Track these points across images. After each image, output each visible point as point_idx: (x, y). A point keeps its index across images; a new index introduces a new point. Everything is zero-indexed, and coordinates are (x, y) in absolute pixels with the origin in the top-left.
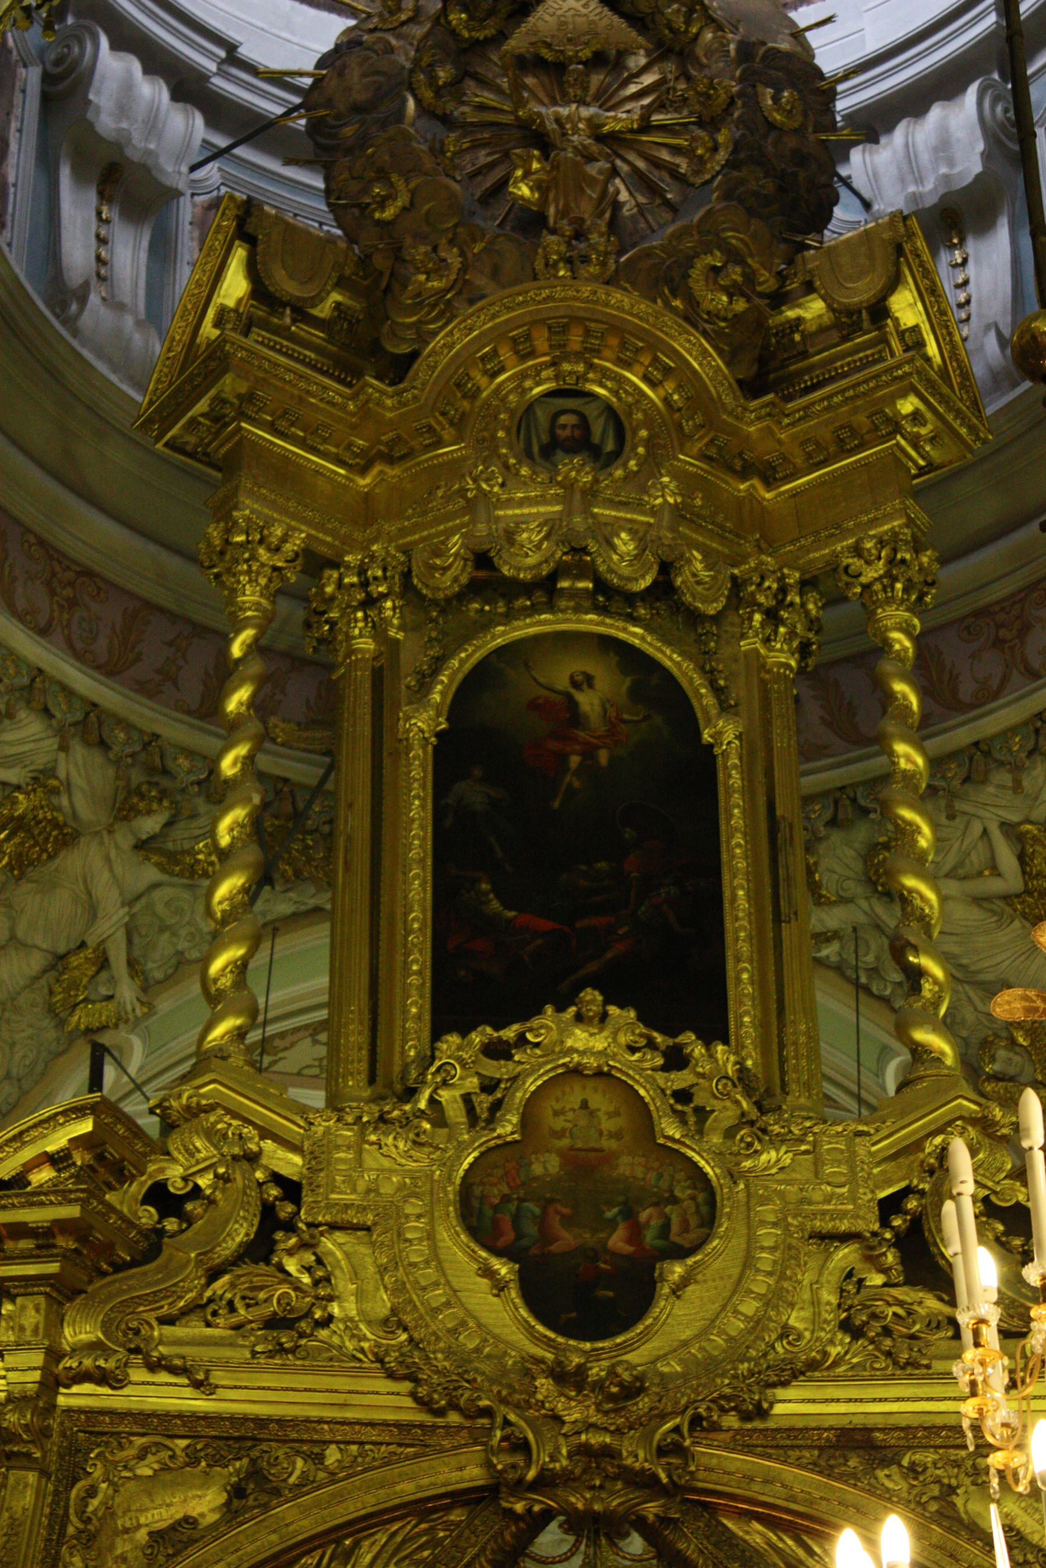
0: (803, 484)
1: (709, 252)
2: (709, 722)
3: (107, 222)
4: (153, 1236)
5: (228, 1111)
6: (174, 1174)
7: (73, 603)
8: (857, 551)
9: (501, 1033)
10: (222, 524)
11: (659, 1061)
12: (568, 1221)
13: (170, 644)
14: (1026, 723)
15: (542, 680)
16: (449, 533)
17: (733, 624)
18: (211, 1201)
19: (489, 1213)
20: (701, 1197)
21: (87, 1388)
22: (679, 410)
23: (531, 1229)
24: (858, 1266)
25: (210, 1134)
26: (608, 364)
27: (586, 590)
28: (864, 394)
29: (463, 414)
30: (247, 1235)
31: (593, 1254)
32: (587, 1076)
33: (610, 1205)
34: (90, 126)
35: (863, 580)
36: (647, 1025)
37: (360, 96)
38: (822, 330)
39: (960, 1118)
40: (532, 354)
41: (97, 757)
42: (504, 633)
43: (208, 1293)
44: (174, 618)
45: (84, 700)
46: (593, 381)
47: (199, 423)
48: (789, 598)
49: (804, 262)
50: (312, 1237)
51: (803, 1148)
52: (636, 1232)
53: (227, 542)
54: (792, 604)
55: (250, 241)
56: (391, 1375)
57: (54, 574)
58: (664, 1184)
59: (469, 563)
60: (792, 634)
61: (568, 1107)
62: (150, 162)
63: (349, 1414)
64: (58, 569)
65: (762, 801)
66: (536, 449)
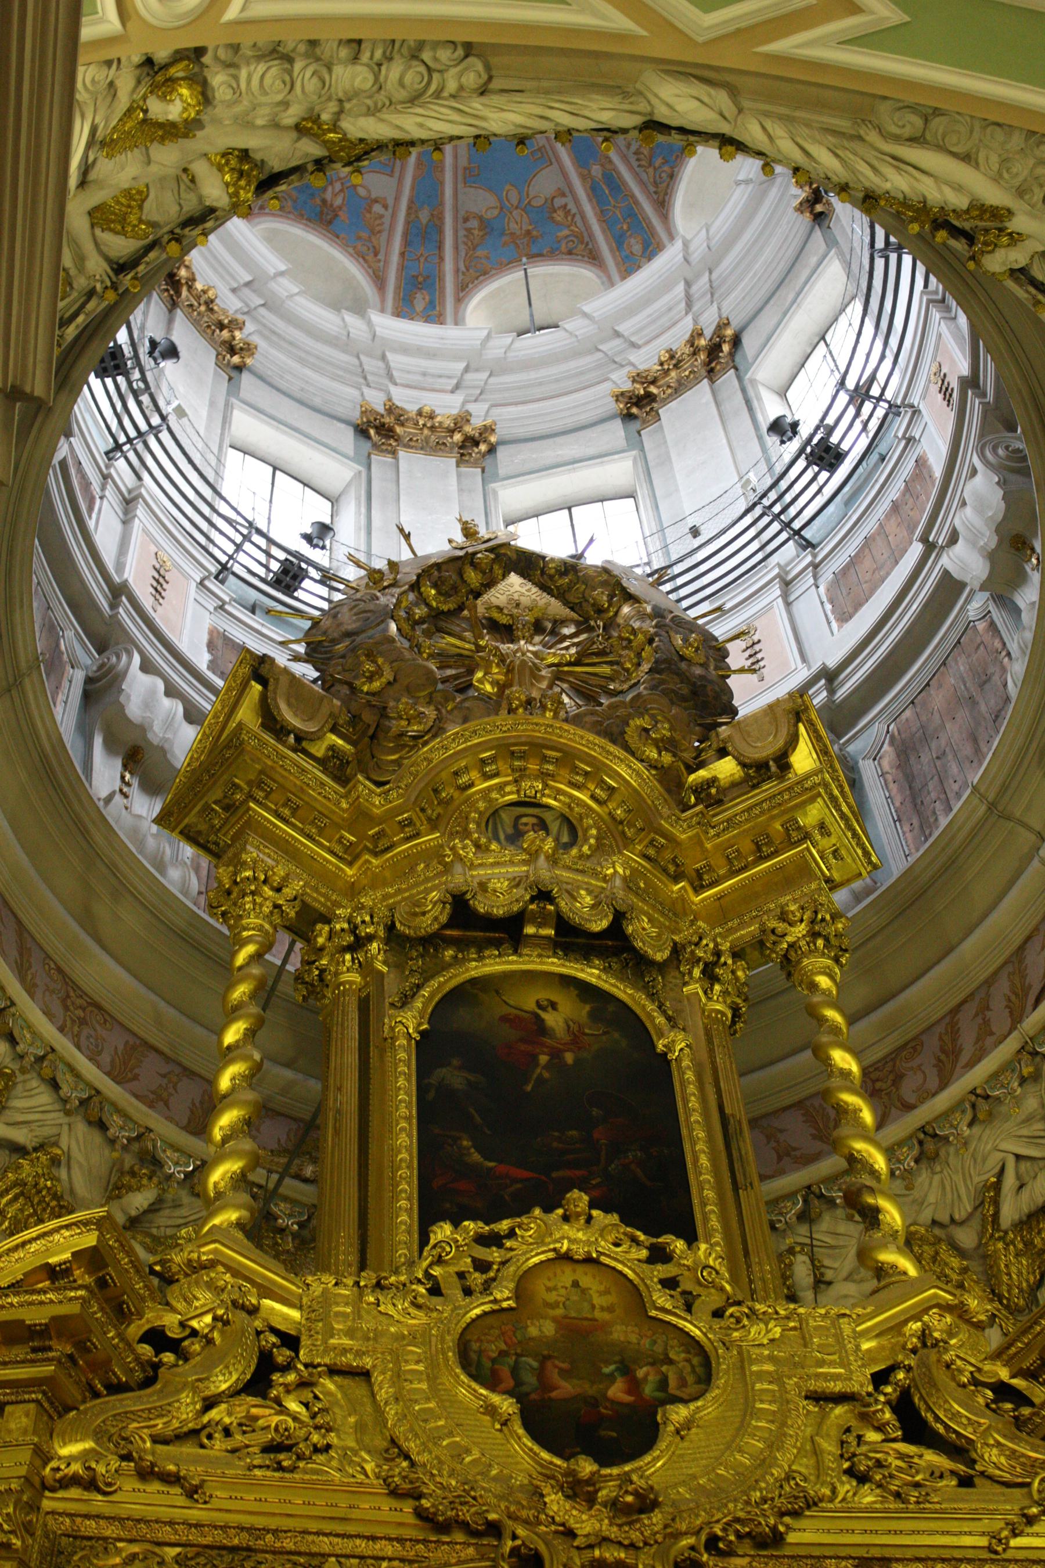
0: (726, 888)
1: (641, 715)
2: (661, 1035)
3: (128, 784)
4: (149, 1369)
5: (229, 1269)
6: (170, 1321)
7: (83, 1022)
8: (783, 917)
9: (492, 1226)
10: (231, 868)
11: (644, 1253)
12: (565, 1374)
13: (164, 1076)
14: (910, 1137)
15: (512, 1003)
16: (428, 891)
17: (675, 978)
18: (210, 1341)
19: (488, 1364)
20: (696, 1361)
21: (74, 1492)
22: (621, 822)
23: (530, 1379)
24: (853, 1423)
25: (210, 1286)
26: (562, 786)
27: (547, 938)
28: (780, 804)
29: (439, 815)
30: (244, 1373)
31: (593, 1402)
32: (578, 1261)
33: (607, 1363)
34: (122, 708)
35: (790, 939)
36: (627, 1225)
37: (351, 627)
38: (734, 785)
39: (937, 1306)
40: (497, 775)
41: (97, 1137)
42: (476, 968)
43: (206, 1419)
44: (168, 1059)
45: (89, 1085)
46: (549, 796)
47: (213, 810)
48: (723, 959)
49: (717, 735)
50: (311, 1375)
51: (792, 1324)
52: (634, 1385)
53: (235, 883)
54: (725, 963)
55: (263, 682)
56: (394, 1493)
57: (68, 996)
58: (659, 1348)
59: (448, 906)
60: (725, 993)
61: (560, 1285)
62: (167, 746)
63: (351, 1529)
64: (72, 994)
65: (712, 1098)
66: (502, 837)
